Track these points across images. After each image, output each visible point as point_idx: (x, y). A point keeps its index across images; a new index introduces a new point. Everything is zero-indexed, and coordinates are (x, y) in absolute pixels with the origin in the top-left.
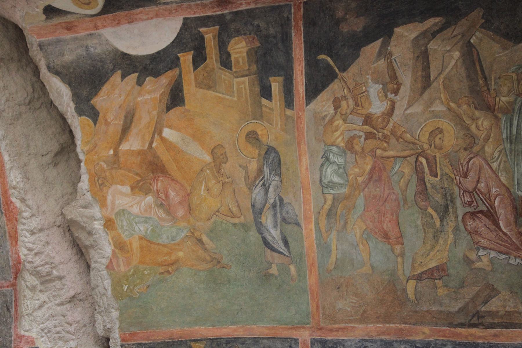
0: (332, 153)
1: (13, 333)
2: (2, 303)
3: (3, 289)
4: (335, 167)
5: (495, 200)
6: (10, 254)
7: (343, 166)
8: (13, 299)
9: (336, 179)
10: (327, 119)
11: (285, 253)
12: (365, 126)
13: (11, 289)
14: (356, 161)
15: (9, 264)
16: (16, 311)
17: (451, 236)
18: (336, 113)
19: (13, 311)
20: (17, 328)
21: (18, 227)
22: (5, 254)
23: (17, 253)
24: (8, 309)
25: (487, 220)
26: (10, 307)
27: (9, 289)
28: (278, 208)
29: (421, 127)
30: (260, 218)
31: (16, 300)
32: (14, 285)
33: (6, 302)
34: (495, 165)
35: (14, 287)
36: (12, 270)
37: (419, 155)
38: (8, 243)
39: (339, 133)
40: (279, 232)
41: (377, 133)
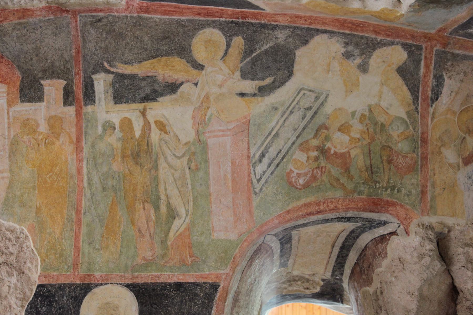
1: (124, 14)
2: (93, 28)
3: (78, 27)
6: (42, 18)
8: (90, 14)
13: (78, 17)
15: (52, 19)
16: (101, 11)
19: (101, 14)
20: (119, 9)
21: (11, 9)
22: (42, 24)
23: (41, 10)
24: (100, 20)
26: (97, 18)
27: (78, 19)
31: (90, 10)
32: (75, 13)
33: (92, 24)
35: (77, 13)
36: (59, 16)
38: (31, 20)
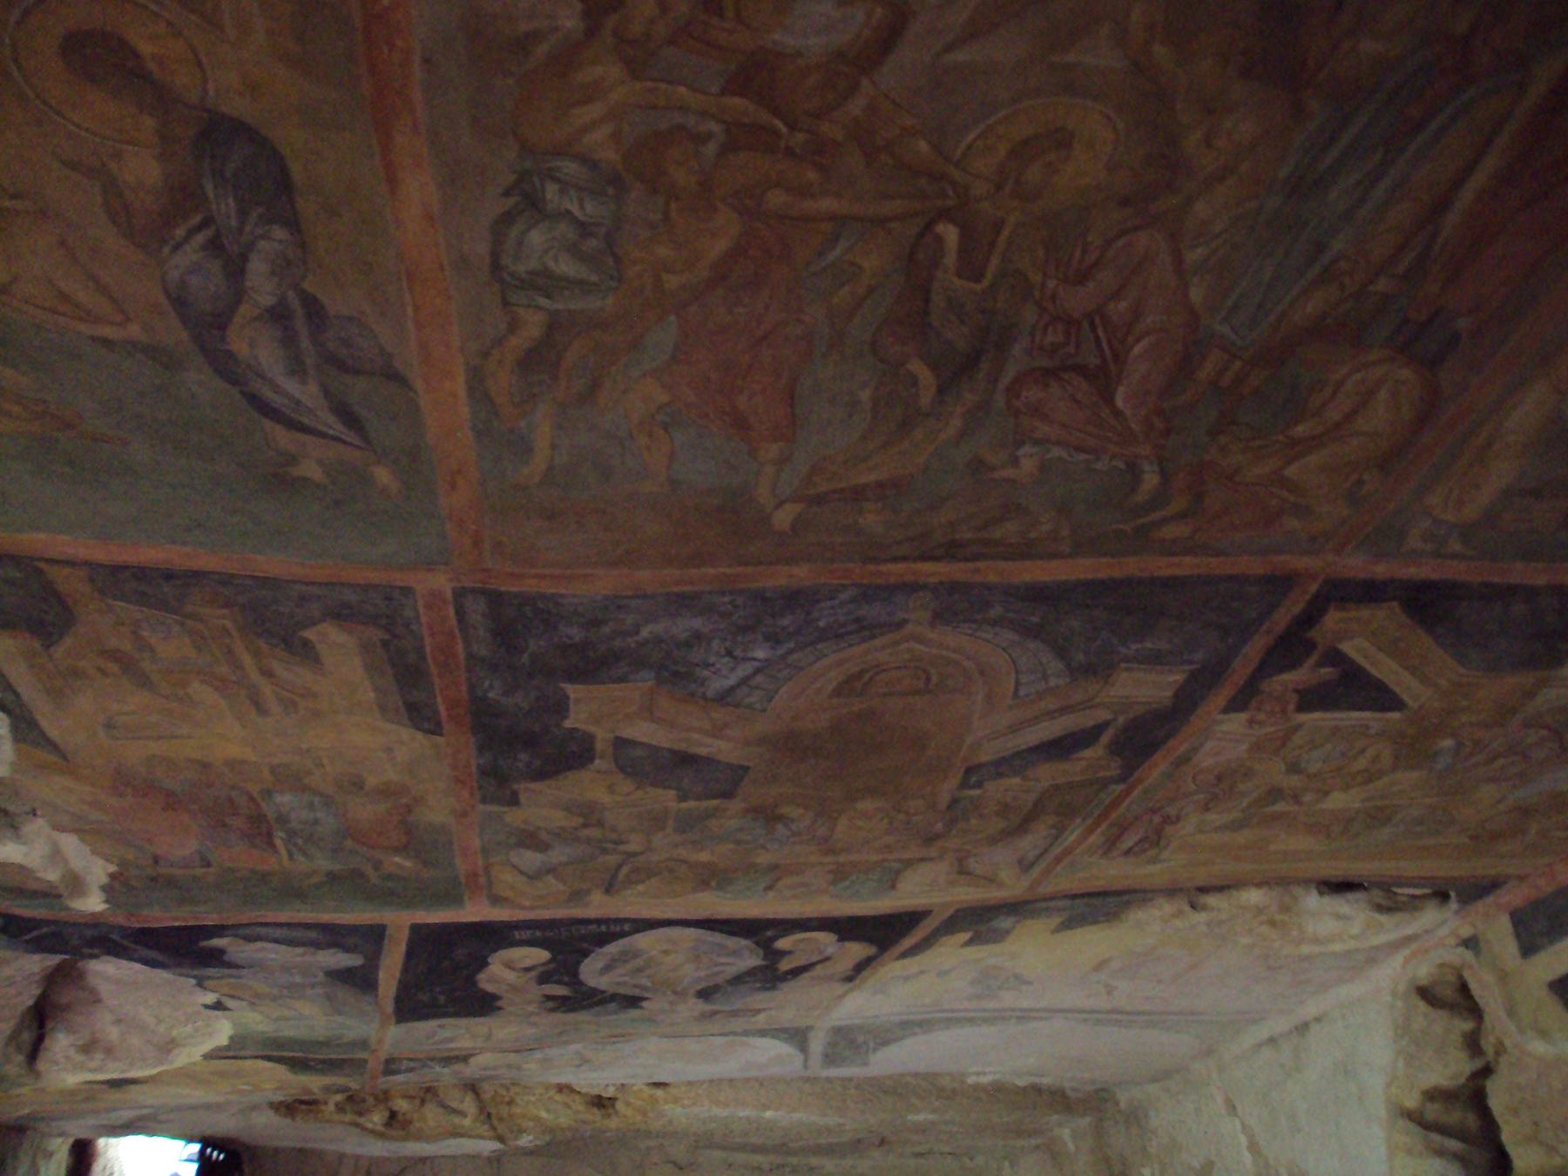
0: (559, 181)
4: (564, 229)
5: (1138, 340)
7: (603, 230)
9: (565, 267)
10: (542, 50)
11: (348, 439)
12: (737, 102)
14: (667, 218)
17: (956, 423)
18: (592, 32)
25: (1085, 386)
28: (300, 325)
29: (991, 121)
30: (223, 339)
34: (1193, 256)
37: (944, 215)
39: (595, 110)
40: (313, 388)
41: (784, 129)
